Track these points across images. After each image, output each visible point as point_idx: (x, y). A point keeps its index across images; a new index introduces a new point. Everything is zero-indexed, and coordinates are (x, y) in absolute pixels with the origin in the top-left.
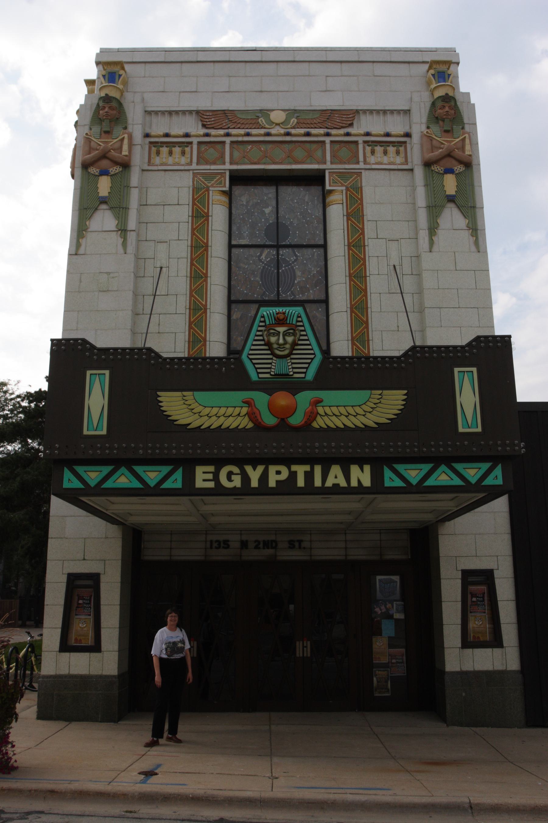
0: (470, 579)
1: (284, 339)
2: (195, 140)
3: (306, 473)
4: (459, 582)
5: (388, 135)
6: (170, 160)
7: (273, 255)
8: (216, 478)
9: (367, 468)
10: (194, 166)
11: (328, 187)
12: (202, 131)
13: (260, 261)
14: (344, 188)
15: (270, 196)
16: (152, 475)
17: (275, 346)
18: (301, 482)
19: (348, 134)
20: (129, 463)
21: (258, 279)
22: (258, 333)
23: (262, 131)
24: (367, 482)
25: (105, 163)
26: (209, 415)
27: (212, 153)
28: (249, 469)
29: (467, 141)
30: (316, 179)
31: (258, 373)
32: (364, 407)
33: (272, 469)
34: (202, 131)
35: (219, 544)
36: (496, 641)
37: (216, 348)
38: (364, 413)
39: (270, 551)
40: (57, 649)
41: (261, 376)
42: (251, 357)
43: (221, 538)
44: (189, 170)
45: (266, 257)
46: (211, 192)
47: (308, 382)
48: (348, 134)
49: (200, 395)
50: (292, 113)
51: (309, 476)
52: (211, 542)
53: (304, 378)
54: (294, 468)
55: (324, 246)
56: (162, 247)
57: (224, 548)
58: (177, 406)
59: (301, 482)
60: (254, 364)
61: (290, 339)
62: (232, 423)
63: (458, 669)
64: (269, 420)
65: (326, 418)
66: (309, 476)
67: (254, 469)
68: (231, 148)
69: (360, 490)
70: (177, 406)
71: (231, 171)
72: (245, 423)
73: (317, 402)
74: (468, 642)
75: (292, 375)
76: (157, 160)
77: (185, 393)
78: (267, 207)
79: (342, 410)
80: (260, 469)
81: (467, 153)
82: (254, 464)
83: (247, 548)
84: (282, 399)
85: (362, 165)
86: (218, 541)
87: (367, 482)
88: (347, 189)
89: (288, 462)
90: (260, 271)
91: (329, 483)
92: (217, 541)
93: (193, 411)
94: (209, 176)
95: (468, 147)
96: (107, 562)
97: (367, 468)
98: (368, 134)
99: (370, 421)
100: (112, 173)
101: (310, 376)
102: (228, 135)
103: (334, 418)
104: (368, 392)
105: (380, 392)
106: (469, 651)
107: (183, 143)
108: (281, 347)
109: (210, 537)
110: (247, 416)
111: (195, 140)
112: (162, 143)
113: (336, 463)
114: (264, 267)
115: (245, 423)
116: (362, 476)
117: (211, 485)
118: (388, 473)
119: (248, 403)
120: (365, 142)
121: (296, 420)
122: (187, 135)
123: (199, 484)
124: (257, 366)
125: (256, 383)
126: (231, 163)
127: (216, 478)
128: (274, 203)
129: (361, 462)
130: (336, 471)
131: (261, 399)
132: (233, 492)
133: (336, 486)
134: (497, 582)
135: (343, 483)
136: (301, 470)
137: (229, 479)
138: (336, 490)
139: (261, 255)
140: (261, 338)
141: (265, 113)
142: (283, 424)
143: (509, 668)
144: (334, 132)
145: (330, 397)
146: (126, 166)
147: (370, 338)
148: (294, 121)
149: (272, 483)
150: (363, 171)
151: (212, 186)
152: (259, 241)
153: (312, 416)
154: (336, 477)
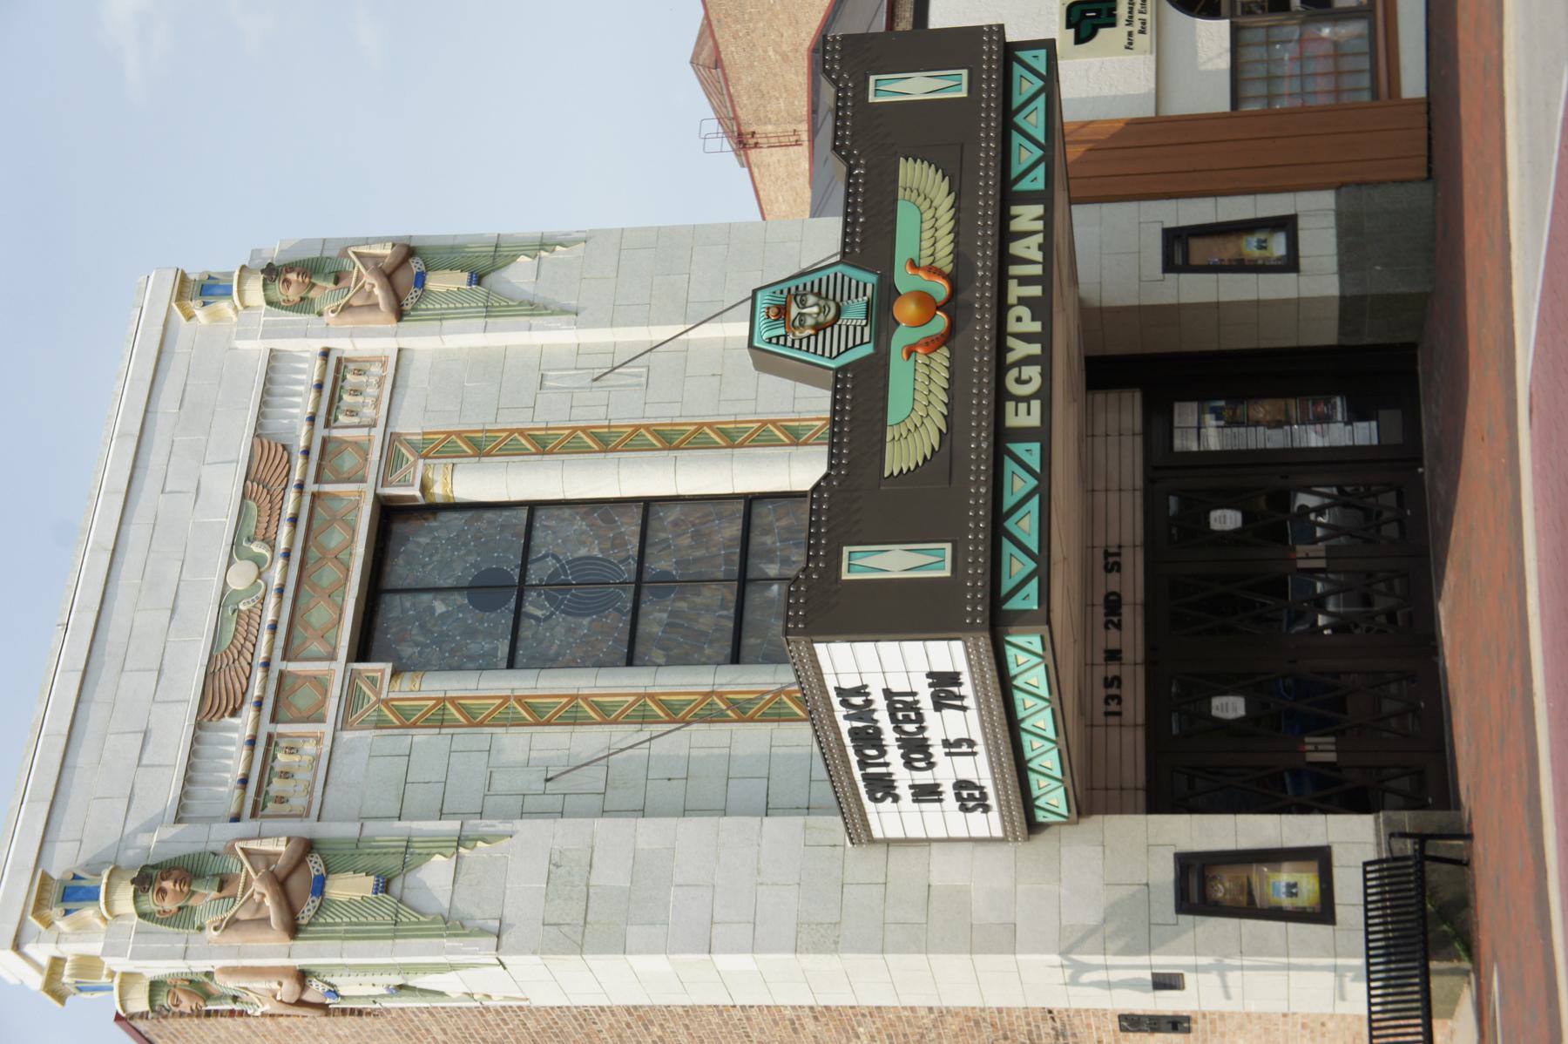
0: (1178, 260)
2: (266, 727)
3: (1020, 284)
4: (1183, 276)
5: (319, 386)
6: (303, 776)
7: (539, 595)
9: (1015, 210)
10: (326, 729)
11: (415, 491)
12: (249, 712)
13: (547, 618)
14: (421, 462)
15: (408, 604)
16: (1018, 484)
17: (821, 318)
18: (1035, 291)
19: (307, 452)
20: (998, 517)
21: (586, 621)
22: (797, 345)
23: (272, 600)
24: (1038, 210)
25: (295, 883)
27: (303, 699)
28: (1011, 357)
29: (364, 250)
30: (391, 516)
32: (923, 208)
33: (1013, 326)
34: (249, 712)
35: (1113, 697)
36: (1287, 224)
37: (815, 403)
39: (1126, 611)
40: (1330, 928)
41: (866, 339)
42: (835, 353)
43: (1100, 692)
44: (334, 739)
45: (542, 607)
46: (392, 695)
47: (881, 279)
48: (307, 452)
49: (893, 416)
50: (236, 548)
51: (1024, 281)
52: (1107, 714)
54: (1012, 299)
55: (533, 506)
56: (500, 784)
57: (1119, 686)
58: (908, 444)
59: (1035, 291)
60: (847, 349)
61: (811, 299)
62: (941, 376)
63: (1336, 278)
64: (940, 322)
66: (1024, 281)
67: (1011, 350)
68: (296, 659)
69: (1047, 218)
70: (908, 444)
71: (349, 660)
72: (941, 357)
73: (913, 264)
74: (1290, 264)
76: (298, 802)
77: (889, 438)
78: (432, 609)
79: (927, 235)
80: (1011, 342)
81: (387, 251)
83: (1120, 651)
84: (906, 310)
85: (378, 433)
86: (1107, 700)
87: (1038, 210)
88: (426, 457)
89: (1002, 308)
90: (570, 618)
91: (1038, 256)
92: (1106, 702)
94: (352, 698)
95: (377, 250)
96: (1151, 841)
97: (1015, 210)
98: (312, 419)
99: (944, 202)
100: (322, 870)
101: (870, 279)
102: (267, 665)
103: (939, 245)
104: (901, 204)
105: (901, 191)
106: (1303, 263)
107: (267, 751)
108: (822, 310)
109: (1099, 718)
111: (266, 727)
112: (258, 793)
113: (1007, 248)
114: (563, 612)
115: (941, 357)
116: (1027, 217)
117: (1036, 405)
118: (1025, 185)
119: (910, 351)
120: (327, 425)
121: (940, 289)
122: (252, 742)
123: (1034, 420)
124: (850, 344)
125: (876, 346)
126: (332, 657)
127: (1027, 399)
128: (425, 597)
129: (1005, 217)
130: (1017, 248)
131: (903, 337)
132: (1047, 376)
133: (1041, 247)
134: (1184, 222)
135: (1039, 238)
136: (1015, 291)
138: (1045, 247)
139: (537, 618)
140: (805, 342)
141: (226, 598)
142: (948, 306)
143: (1333, 206)
144: (296, 476)
145: (904, 248)
146: (309, 846)
147: (732, 419)
148: (257, 548)
149: (1036, 327)
150: (389, 431)
151: (378, 694)
152: (507, 621)
153: (933, 270)
154: (1028, 248)
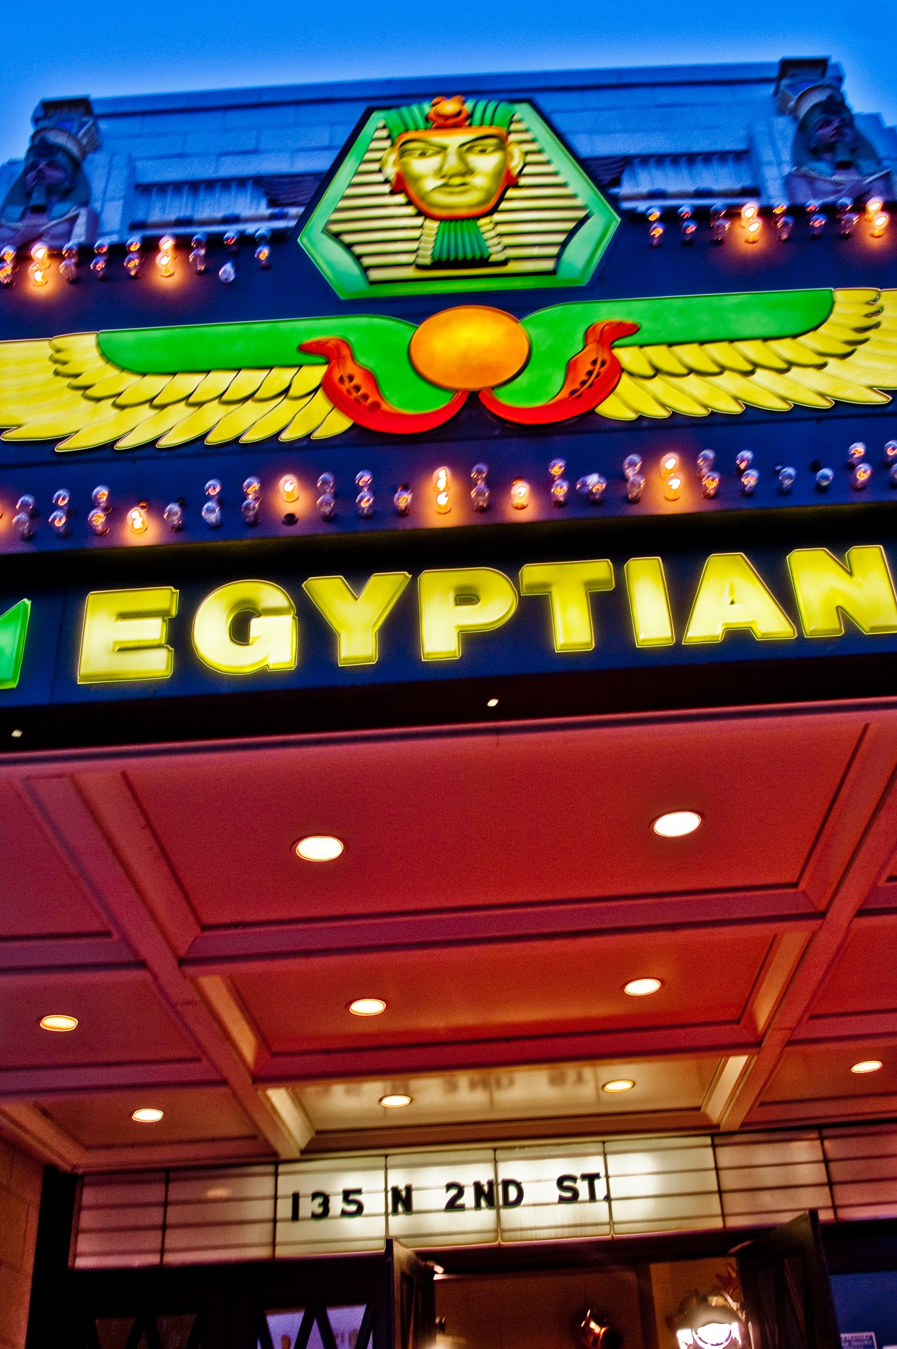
1: (462, 159)
8: (180, 634)
18: (572, 629)
26: (156, 402)
28: (328, 591)
31: (366, 269)
38: (820, 360)
42: (335, 228)
53: (553, 272)
54: (534, 574)
59: (572, 629)
60: (349, 247)
65: (657, 385)
75: (504, 263)
80: (384, 589)
82: (356, 567)
93: (90, 392)
110: (320, 393)
124: (358, 250)
127: (180, 634)
137: (240, 631)
